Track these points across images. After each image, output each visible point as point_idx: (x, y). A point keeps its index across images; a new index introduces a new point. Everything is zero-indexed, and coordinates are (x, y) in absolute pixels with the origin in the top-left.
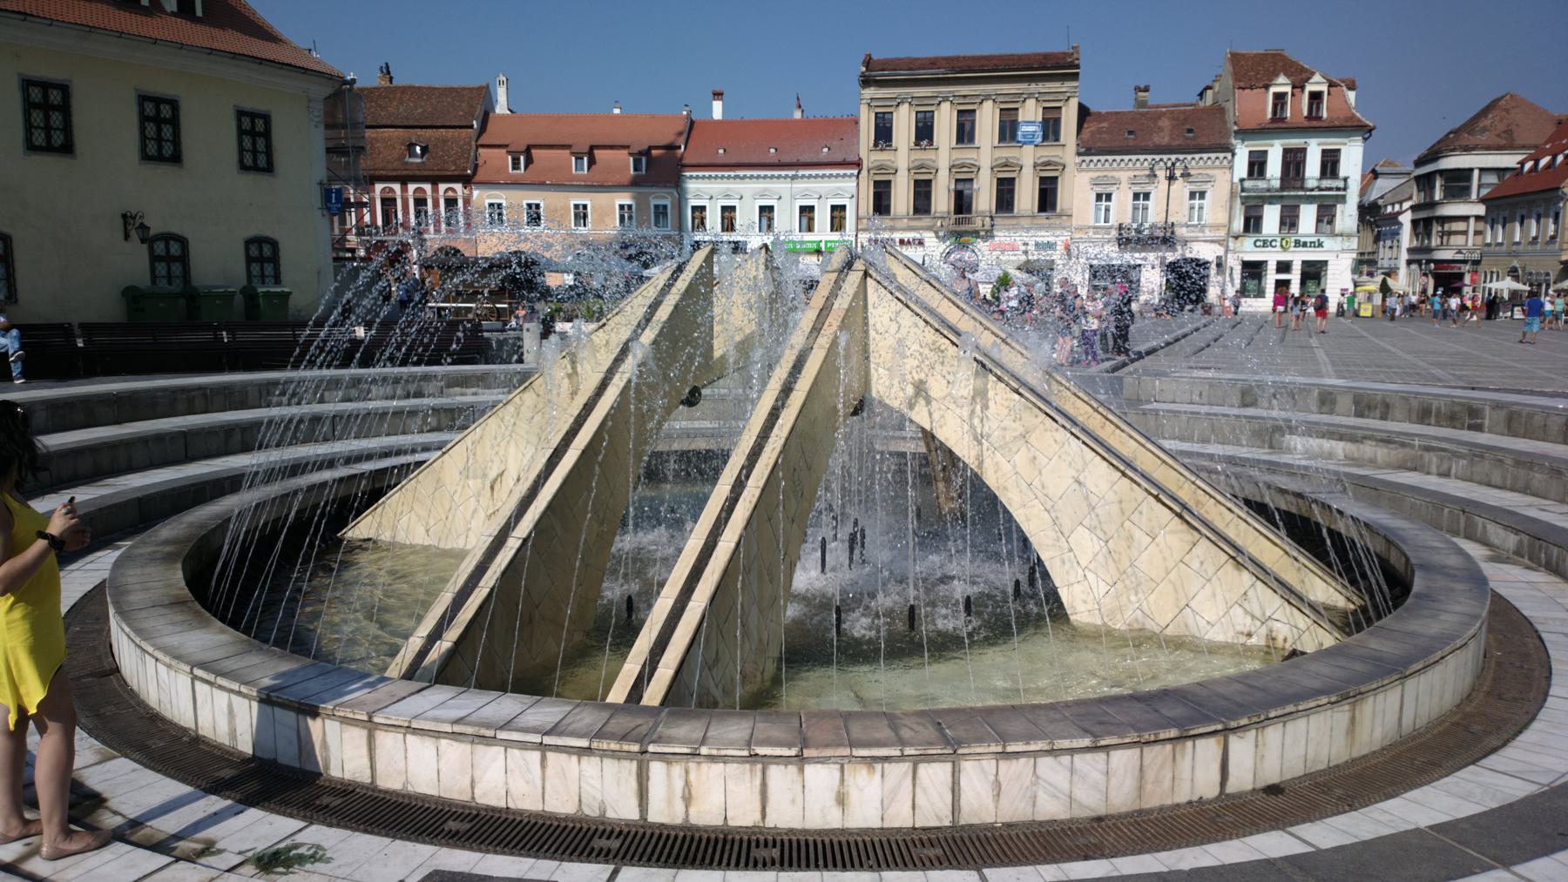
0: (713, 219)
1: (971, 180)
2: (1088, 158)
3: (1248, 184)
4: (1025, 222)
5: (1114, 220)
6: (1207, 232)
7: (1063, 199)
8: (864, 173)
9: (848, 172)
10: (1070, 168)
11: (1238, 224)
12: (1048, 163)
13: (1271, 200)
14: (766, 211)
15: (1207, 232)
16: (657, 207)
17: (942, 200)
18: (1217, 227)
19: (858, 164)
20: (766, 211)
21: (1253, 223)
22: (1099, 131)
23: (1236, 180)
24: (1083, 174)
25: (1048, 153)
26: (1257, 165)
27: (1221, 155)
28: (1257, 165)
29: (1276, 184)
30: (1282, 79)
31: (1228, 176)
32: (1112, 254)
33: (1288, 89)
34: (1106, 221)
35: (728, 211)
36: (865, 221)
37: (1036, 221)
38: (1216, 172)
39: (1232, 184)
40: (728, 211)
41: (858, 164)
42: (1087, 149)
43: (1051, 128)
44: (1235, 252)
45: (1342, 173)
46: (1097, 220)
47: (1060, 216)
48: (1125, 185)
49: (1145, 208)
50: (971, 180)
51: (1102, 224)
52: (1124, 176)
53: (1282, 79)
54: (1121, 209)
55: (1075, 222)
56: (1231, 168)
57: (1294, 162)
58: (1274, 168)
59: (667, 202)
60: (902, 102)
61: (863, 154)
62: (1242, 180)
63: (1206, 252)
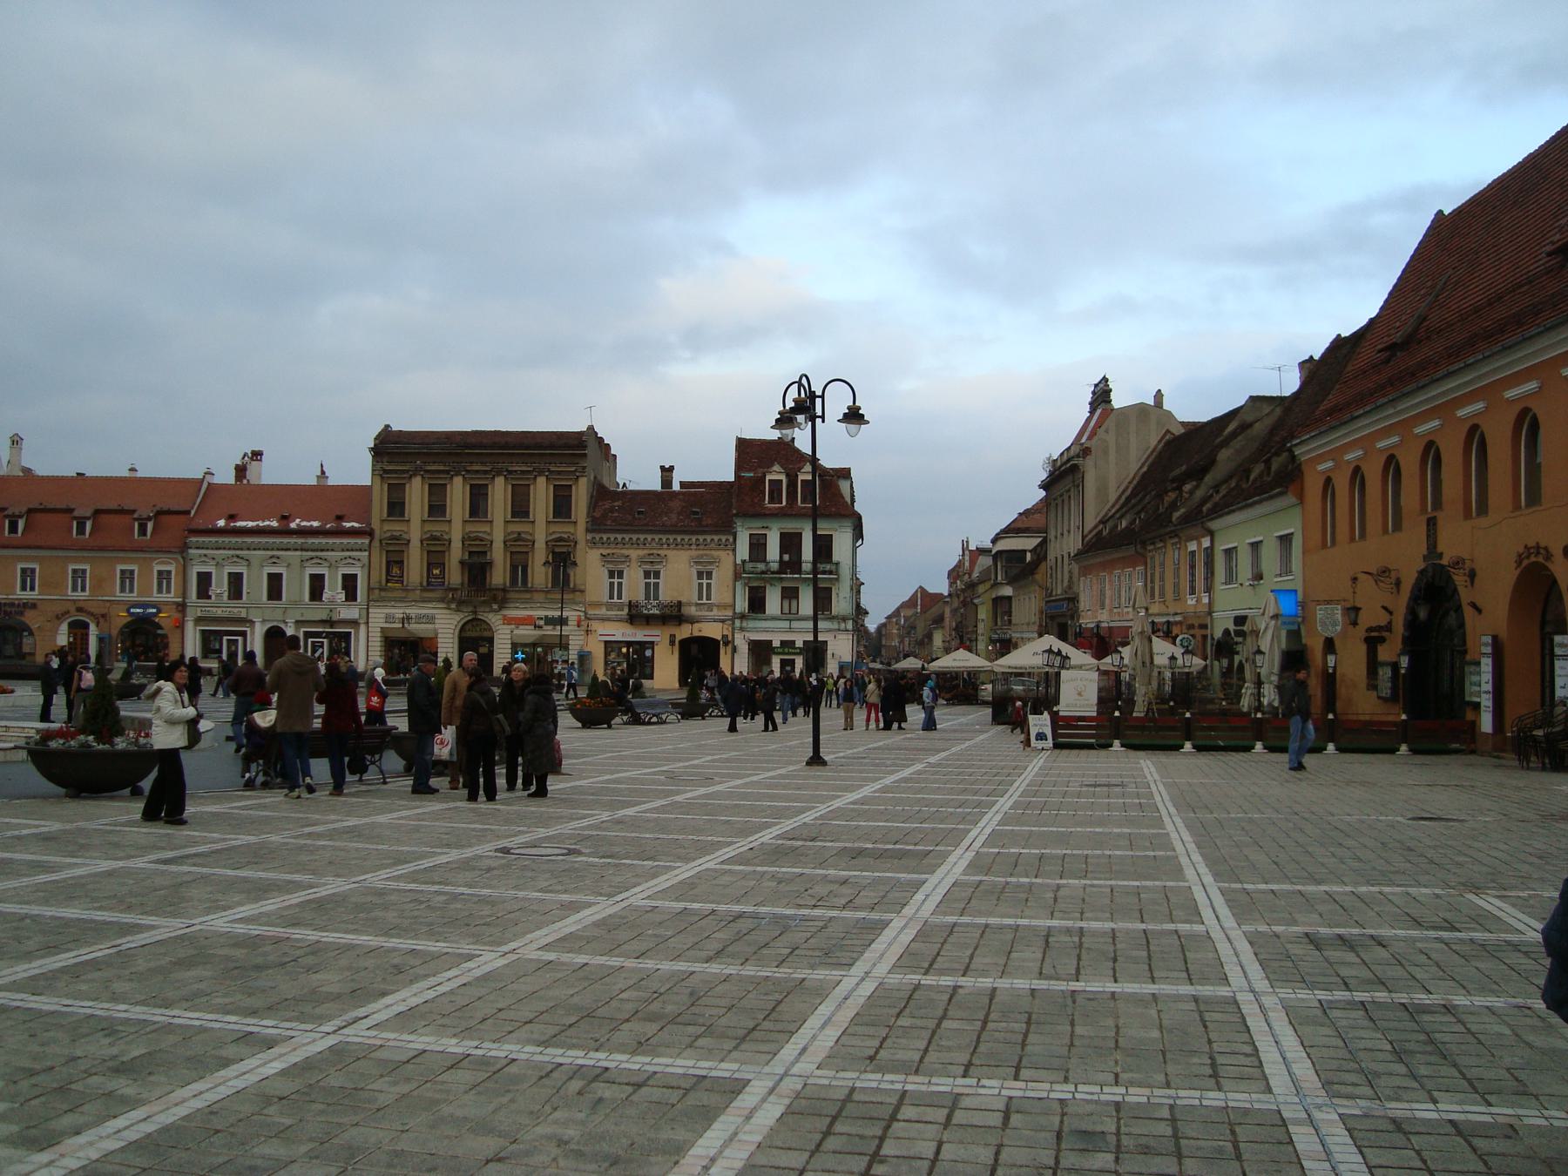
0: (220, 587)
1: (485, 553)
2: (598, 537)
3: (749, 566)
4: (540, 597)
5: (625, 599)
6: (715, 609)
7: (576, 576)
8: (376, 543)
9: (359, 541)
10: (581, 545)
11: (742, 605)
12: (560, 539)
13: (771, 582)
14: (275, 583)
15: (715, 609)
16: (160, 573)
17: (455, 576)
18: (725, 607)
19: (370, 533)
20: (275, 583)
21: (757, 604)
22: (612, 510)
23: (739, 562)
24: (595, 550)
25: (562, 529)
26: (758, 546)
27: (724, 538)
28: (758, 546)
29: (775, 566)
30: (777, 468)
31: (732, 557)
32: (622, 633)
33: (783, 477)
34: (620, 597)
35: (236, 581)
36: (377, 592)
37: (549, 596)
38: (722, 554)
39: (736, 565)
40: (236, 581)
41: (370, 533)
42: (597, 524)
43: (562, 507)
44: (742, 629)
45: (835, 558)
46: (611, 597)
47: (574, 591)
48: (634, 564)
49: (656, 585)
50: (485, 553)
51: (615, 600)
52: (635, 554)
53: (777, 468)
54: (633, 585)
55: (591, 596)
56: (734, 550)
57: (790, 543)
58: (773, 551)
59: (172, 568)
60: (415, 475)
61: (376, 524)
62: (744, 562)
63: (713, 631)
